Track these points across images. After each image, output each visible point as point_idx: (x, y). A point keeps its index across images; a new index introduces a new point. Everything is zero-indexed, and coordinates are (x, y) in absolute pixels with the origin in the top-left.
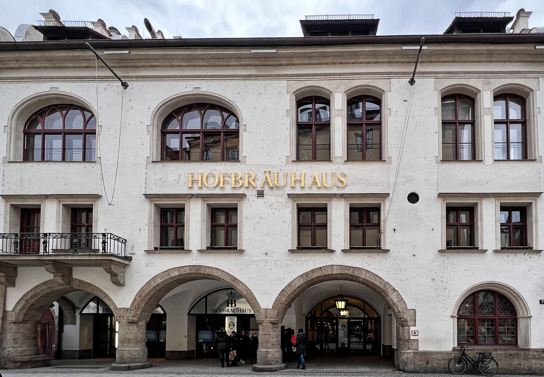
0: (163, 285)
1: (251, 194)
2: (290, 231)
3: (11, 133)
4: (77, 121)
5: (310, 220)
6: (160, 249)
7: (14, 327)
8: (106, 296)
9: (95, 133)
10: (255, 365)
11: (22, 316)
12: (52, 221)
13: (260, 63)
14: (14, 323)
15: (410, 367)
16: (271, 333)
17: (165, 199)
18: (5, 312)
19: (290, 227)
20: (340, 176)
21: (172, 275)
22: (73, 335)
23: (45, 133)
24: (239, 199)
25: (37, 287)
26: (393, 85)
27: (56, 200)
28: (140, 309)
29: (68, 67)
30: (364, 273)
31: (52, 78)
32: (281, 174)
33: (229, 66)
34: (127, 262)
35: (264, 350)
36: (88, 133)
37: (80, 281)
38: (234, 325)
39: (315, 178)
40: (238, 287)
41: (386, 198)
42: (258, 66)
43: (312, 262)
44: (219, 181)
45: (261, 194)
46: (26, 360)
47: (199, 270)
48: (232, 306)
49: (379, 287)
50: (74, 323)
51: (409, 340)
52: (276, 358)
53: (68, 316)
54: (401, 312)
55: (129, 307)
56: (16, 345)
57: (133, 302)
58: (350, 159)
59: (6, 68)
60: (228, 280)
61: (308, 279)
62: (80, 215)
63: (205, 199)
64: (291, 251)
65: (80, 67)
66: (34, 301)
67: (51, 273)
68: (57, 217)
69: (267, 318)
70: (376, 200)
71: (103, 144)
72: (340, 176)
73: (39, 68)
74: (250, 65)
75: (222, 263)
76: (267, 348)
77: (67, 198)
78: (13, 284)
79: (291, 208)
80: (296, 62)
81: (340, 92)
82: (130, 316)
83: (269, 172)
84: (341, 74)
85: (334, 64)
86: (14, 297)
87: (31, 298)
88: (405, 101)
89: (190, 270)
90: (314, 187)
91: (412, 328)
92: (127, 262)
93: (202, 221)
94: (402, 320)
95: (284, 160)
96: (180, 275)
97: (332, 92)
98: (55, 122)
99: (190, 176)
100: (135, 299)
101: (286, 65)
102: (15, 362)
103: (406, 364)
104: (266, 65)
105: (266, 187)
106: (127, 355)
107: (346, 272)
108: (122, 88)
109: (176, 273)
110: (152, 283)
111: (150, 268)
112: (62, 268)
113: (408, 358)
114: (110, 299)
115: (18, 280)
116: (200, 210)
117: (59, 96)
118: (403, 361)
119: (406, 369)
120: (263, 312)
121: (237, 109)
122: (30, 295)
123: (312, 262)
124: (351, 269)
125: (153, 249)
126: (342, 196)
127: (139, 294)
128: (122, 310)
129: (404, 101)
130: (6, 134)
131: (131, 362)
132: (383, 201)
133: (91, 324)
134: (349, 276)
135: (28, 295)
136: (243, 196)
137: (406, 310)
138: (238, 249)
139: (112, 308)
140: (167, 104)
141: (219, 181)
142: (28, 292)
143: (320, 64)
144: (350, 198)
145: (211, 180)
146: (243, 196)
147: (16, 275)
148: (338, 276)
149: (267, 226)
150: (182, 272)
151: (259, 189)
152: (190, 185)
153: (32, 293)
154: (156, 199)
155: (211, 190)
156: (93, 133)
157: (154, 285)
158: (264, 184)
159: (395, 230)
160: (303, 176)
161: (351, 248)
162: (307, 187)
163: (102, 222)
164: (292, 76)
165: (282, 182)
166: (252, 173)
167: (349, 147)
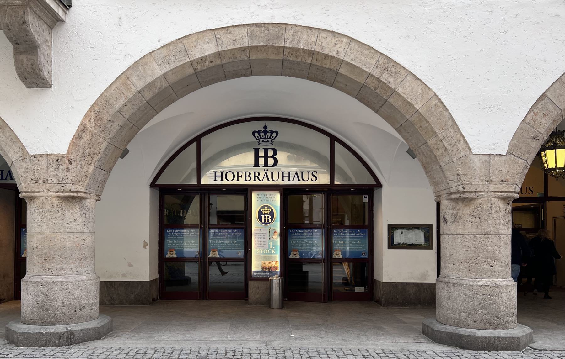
0: (165, 84)
21: (196, 54)
35: (483, 282)
47: (278, 38)
57: (78, 137)
89: (251, 36)
100: (83, 129)
110: (134, 79)
120: (477, 163)
127: (96, 112)
128: (44, 162)
150: (227, 43)
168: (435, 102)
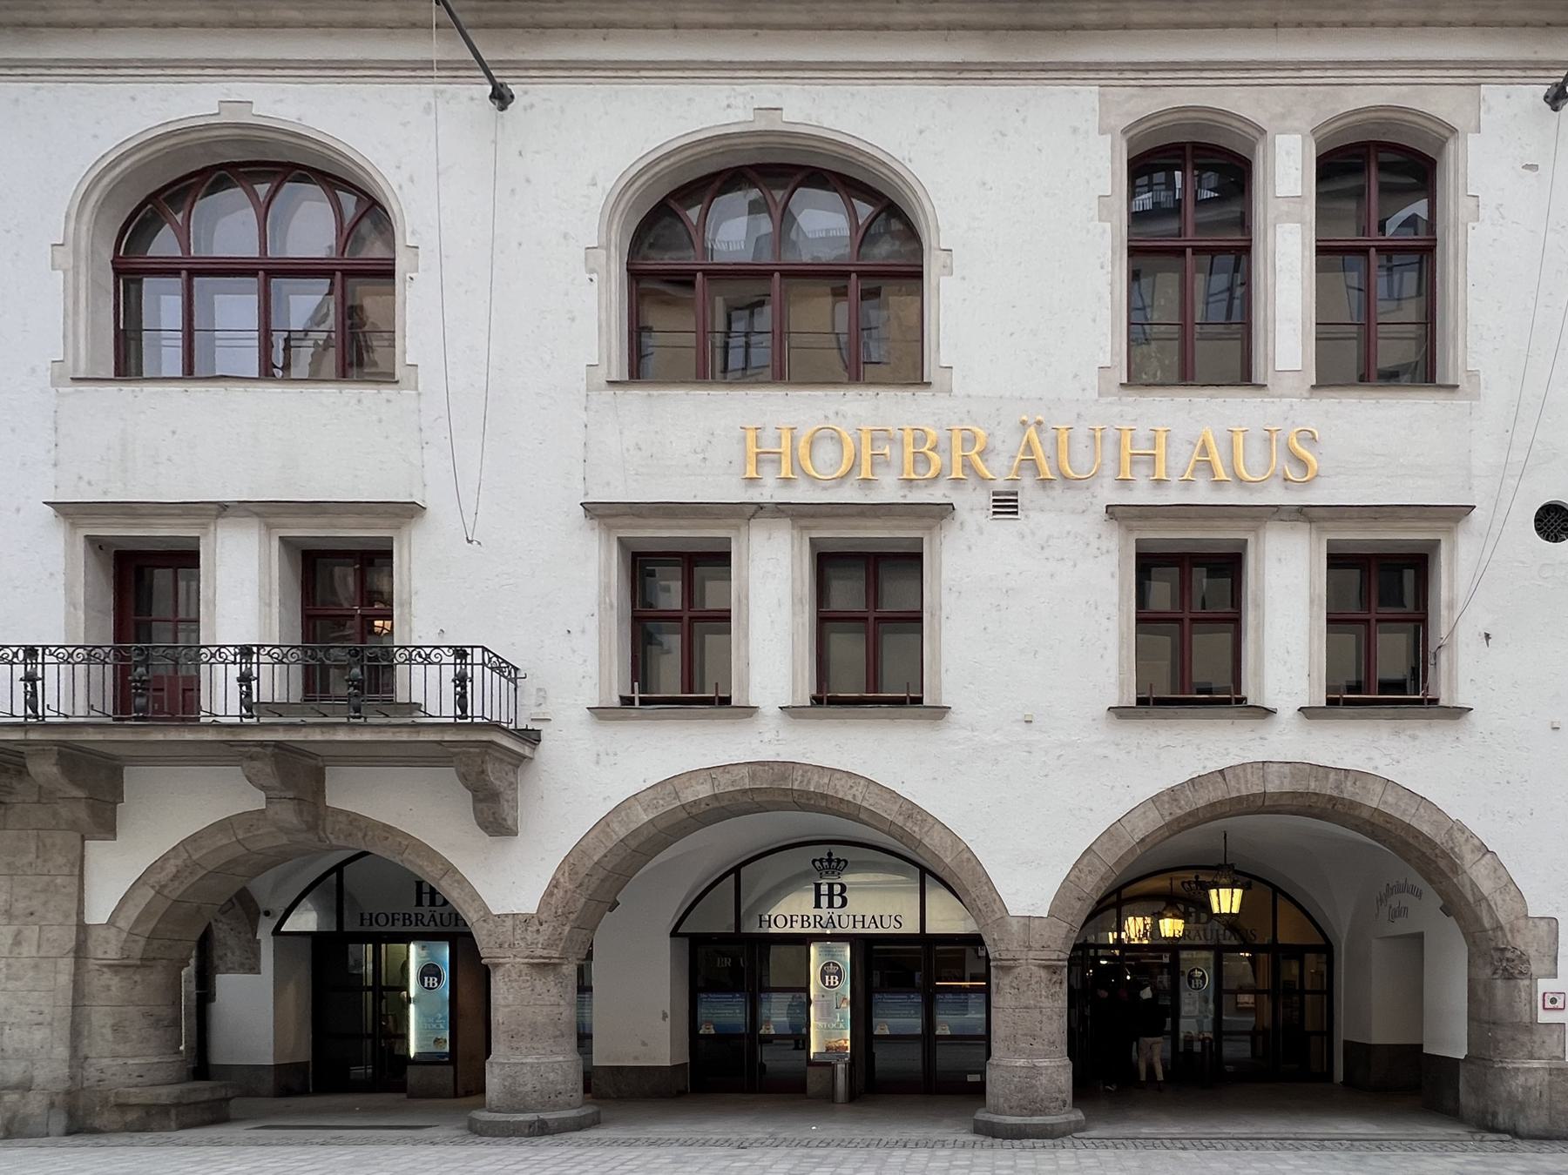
1: (972, 505)
2: (1112, 640)
3: (76, 268)
4: (310, 227)
5: (1187, 596)
6: (643, 702)
7: (115, 981)
8: (450, 869)
9: (390, 274)
10: (981, 1115)
11: (142, 942)
12: (242, 598)
13: (1003, 19)
14: (115, 968)
15: (1537, 1120)
16: (1046, 1003)
17: (662, 522)
18: (83, 928)
19: (1113, 625)
20: (1294, 442)
21: (689, 796)
22: (254, 1011)
23: (196, 271)
24: (929, 522)
25: (194, 838)
26: (1489, 109)
27: (256, 520)
28: (572, 917)
29: (284, 25)
30: (1379, 789)
31: (225, 66)
32: (1081, 432)
33: (886, 27)
34: (526, 751)
35: (1021, 1062)
36: (362, 269)
37: (354, 819)
38: (839, 973)
39: (1204, 450)
40: (926, 841)
41: (1458, 521)
42: (994, 28)
43: (1194, 752)
44: (857, 456)
45: (1006, 505)
46: (164, 1100)
47: (784, 778)
48: (831, 905)
49: (1429, 841)
50: (254, 969)
51: (1532, 1026)
52: (1061, 1092)
53: (231, 942)
54: (1507, 927)
55: (531, 907)
56: (121, 1049)
57: (549, 893)
58: (1327, 379)
59: (49, 25)
60: (891, 813)
61: (1179, 812)
62: (342, 579)
63: (804, 522)
64: (1119, 712)
65: (330, 25)
66: (182, 888)
67: (262, 788)
68: (261, 587)
69: (1030, 948)
70: (1423, 530)
71: (420, 312)
72: (1294, 442)
73: (176, 25)
74: (965, 27)
75: (867, 754)
76: (1031, 1055)
77: (296, 514)
78: (107, 829)
79: (1115, 558)
80: (1137, 17)
81: (1296, 131)
82: (539, 944)
83: (1039, 423)
84: (1299, 66)
85: (1276, 25)
86: (114, 876)
87: (175, 877)
88: (1532, 167)
89: (753, 777)
90: (1202, 482)
91: (1544, 985)
92: (526, 751)
93: (796, 600)
94: (1509, 955)
95: (1092, 379)
96: (715, 796)
97: (1263, 132)
98: (227, 225)
99: (751, 435)
100: (555, 884)
101: (1098, 27)
102: (123, 1107)
103: (1522, 1107)
104: (1024, 28)
105: (1028, 480)
106: (529, 1083)
107: (1313, 786)
108: (491, 106)
109: (703, 791)
110: (616, 826)
111: (602, 770)
112: (297, 772)
113: (1528, 1090)
114: (462, 881)
115: (126, 813)
116: (786, 560)
117: (249, 134)
118: (1511, 1097)
119: (1523, 1125)
120: (1015, 927)
121: (920, 193)
122: (171, 868)
123: (1194, 752)
124: (1332, 775)
125: (616, 701)
126: (1303, 514)
128: (509, 922)
129: (1527, 167)
130: (60, 273)
131: (544, 1106)
132: (1450, 531)
133: (304, 972)
134: (1323, 804)
135: (162, 869)
136: (942, 512)
137: (1522, 922)
138: (926, 702)
139: (471, 916)
140: (657, 169)
141: (857, 456)
142: (164, 858)
143: (1225, 25)
144: (1332, 519)
145: (826, 452)
146: (942, 512)
147: (118, 796)
148: (1285, 801)
149: (1028, 622)
150: (725, 785)
151: (1001, 485)
152: (751, 473)
153: (179, 862)
154: (627, 521)
155: (825, 489)
156: (384, 272)
157: (623, 833)
158: (1019, 468)
159: (1487, 636)
160: (1162, 441)
161: (1330, 702)
162: (1175, 480)
163: (432, 603)
164: (1121, 68)
165: (1080, 462)
166: (976, 429)
167: (1326, 332)
168: (967, 855)
